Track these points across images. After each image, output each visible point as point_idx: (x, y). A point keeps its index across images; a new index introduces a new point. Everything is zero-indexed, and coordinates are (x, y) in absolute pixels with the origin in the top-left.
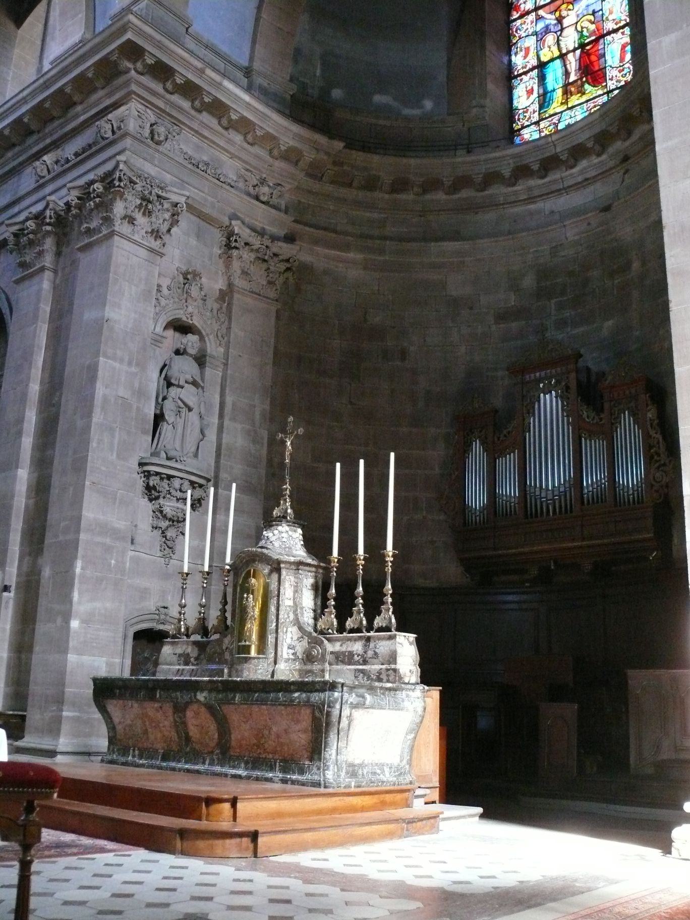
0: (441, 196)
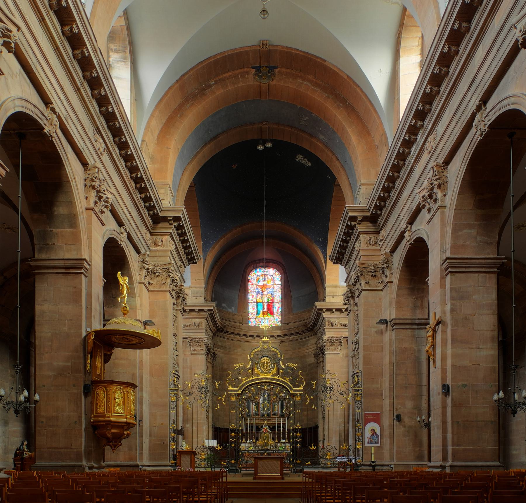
0: (238, 337)
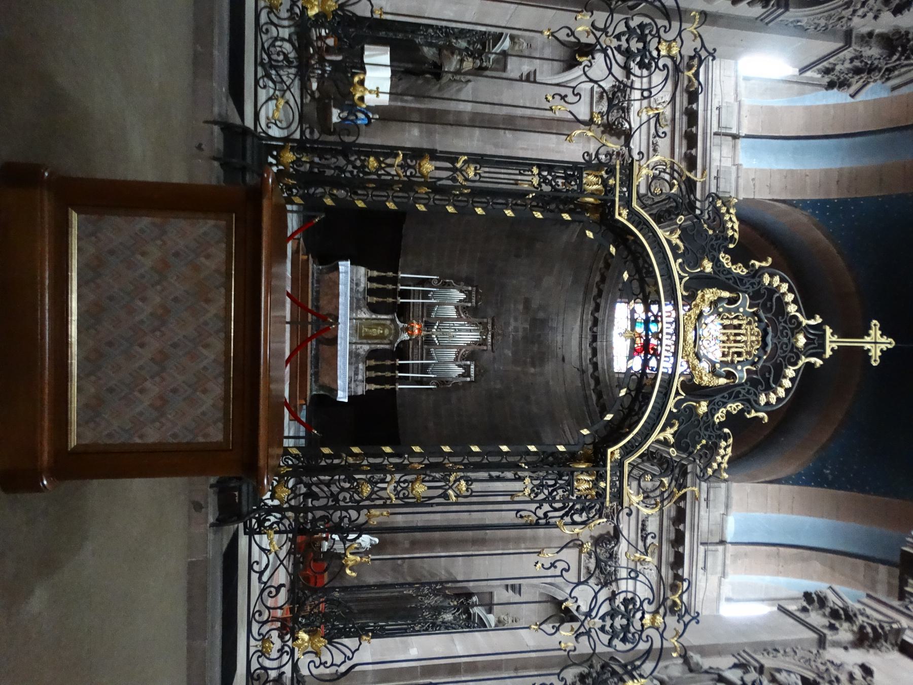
0: (597, 279)
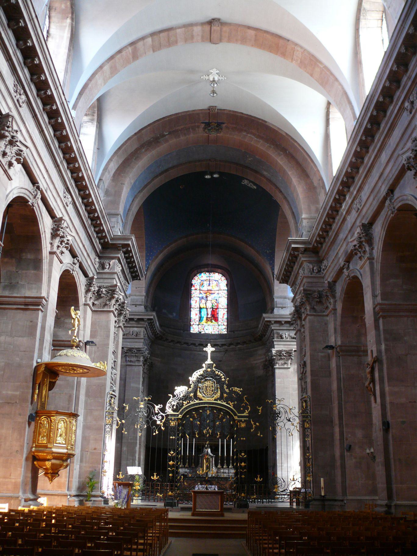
0: (178, 345)
